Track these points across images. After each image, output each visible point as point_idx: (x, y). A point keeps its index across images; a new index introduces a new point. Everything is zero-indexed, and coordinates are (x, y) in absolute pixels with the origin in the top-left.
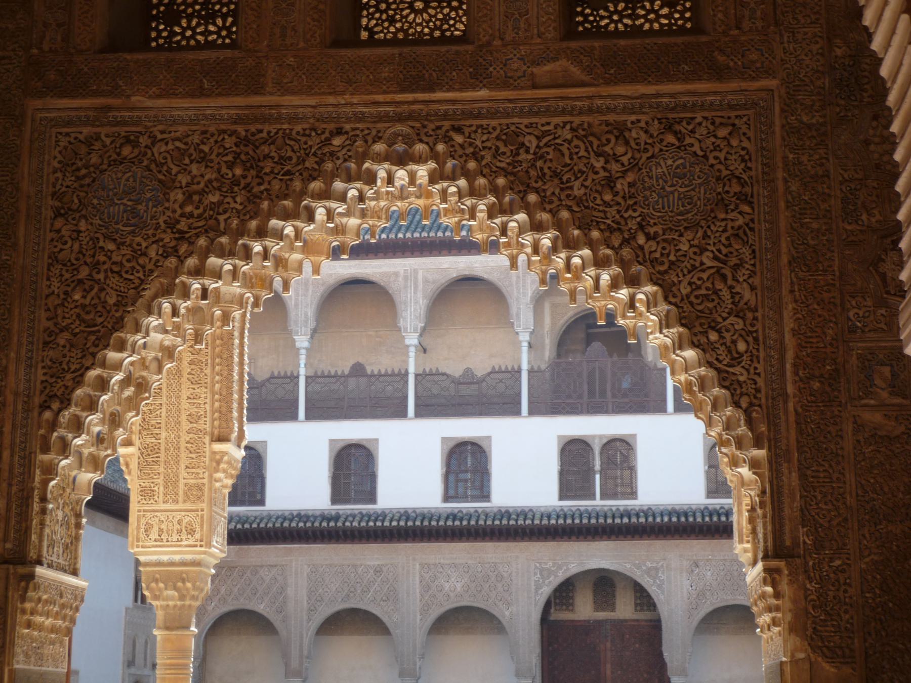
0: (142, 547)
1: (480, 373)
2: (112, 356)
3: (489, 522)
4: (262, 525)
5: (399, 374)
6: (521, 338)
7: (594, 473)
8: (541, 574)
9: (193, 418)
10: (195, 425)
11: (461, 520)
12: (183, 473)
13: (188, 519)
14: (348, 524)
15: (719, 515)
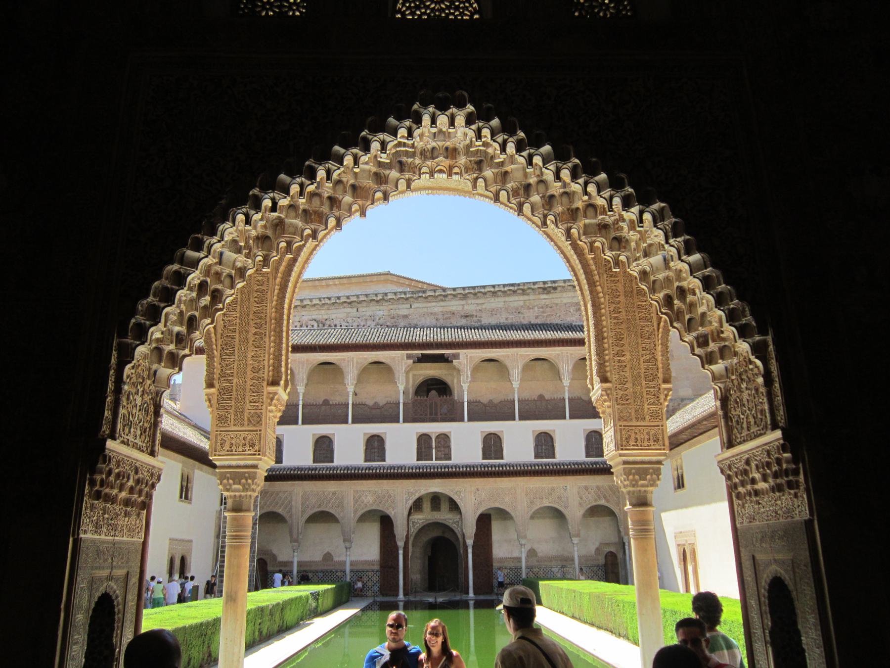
0: (219, 455)
1: (381, 404)
2: (190, 253)
3: (385, 471)
4: (281, 473)
5: (345, 404)
6: (400, 389)
7: (432, 448)
8: (408, 493)
9: (256, 370)
10: (256, 374)
11: (373, 470)
12: (248, 406)
13: (250, 437)
14: (321, 472)
15: (488, 467)
